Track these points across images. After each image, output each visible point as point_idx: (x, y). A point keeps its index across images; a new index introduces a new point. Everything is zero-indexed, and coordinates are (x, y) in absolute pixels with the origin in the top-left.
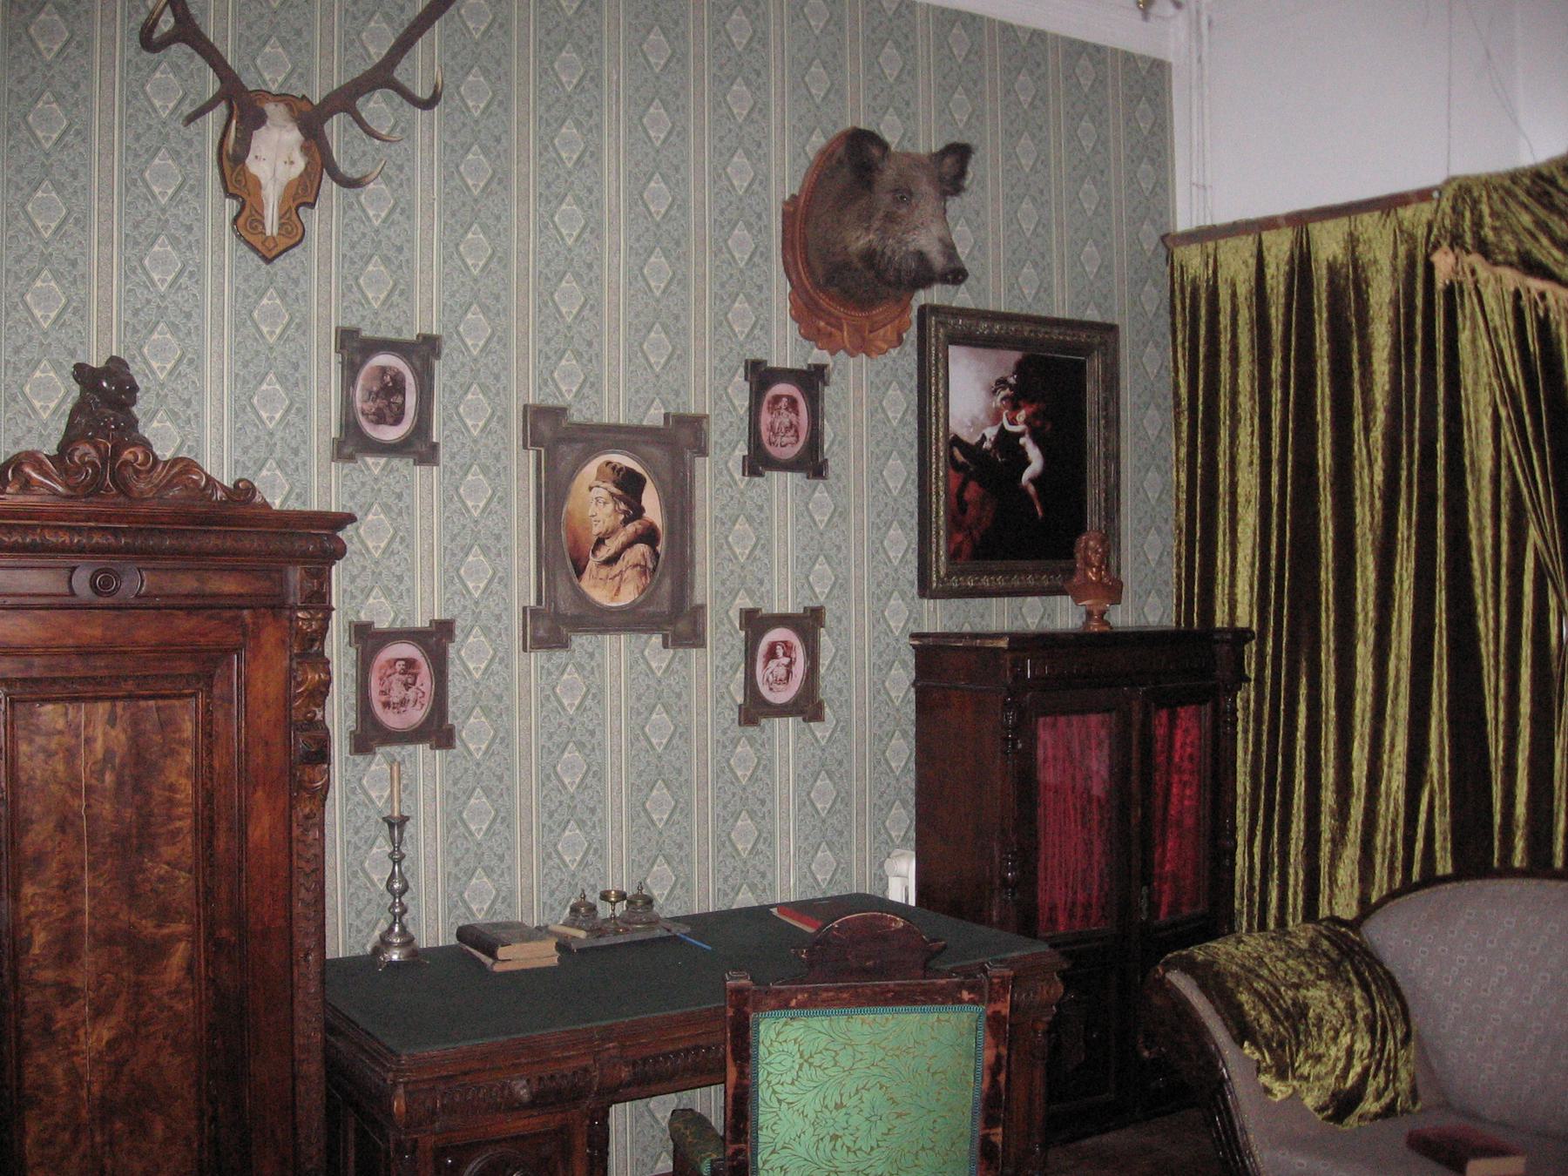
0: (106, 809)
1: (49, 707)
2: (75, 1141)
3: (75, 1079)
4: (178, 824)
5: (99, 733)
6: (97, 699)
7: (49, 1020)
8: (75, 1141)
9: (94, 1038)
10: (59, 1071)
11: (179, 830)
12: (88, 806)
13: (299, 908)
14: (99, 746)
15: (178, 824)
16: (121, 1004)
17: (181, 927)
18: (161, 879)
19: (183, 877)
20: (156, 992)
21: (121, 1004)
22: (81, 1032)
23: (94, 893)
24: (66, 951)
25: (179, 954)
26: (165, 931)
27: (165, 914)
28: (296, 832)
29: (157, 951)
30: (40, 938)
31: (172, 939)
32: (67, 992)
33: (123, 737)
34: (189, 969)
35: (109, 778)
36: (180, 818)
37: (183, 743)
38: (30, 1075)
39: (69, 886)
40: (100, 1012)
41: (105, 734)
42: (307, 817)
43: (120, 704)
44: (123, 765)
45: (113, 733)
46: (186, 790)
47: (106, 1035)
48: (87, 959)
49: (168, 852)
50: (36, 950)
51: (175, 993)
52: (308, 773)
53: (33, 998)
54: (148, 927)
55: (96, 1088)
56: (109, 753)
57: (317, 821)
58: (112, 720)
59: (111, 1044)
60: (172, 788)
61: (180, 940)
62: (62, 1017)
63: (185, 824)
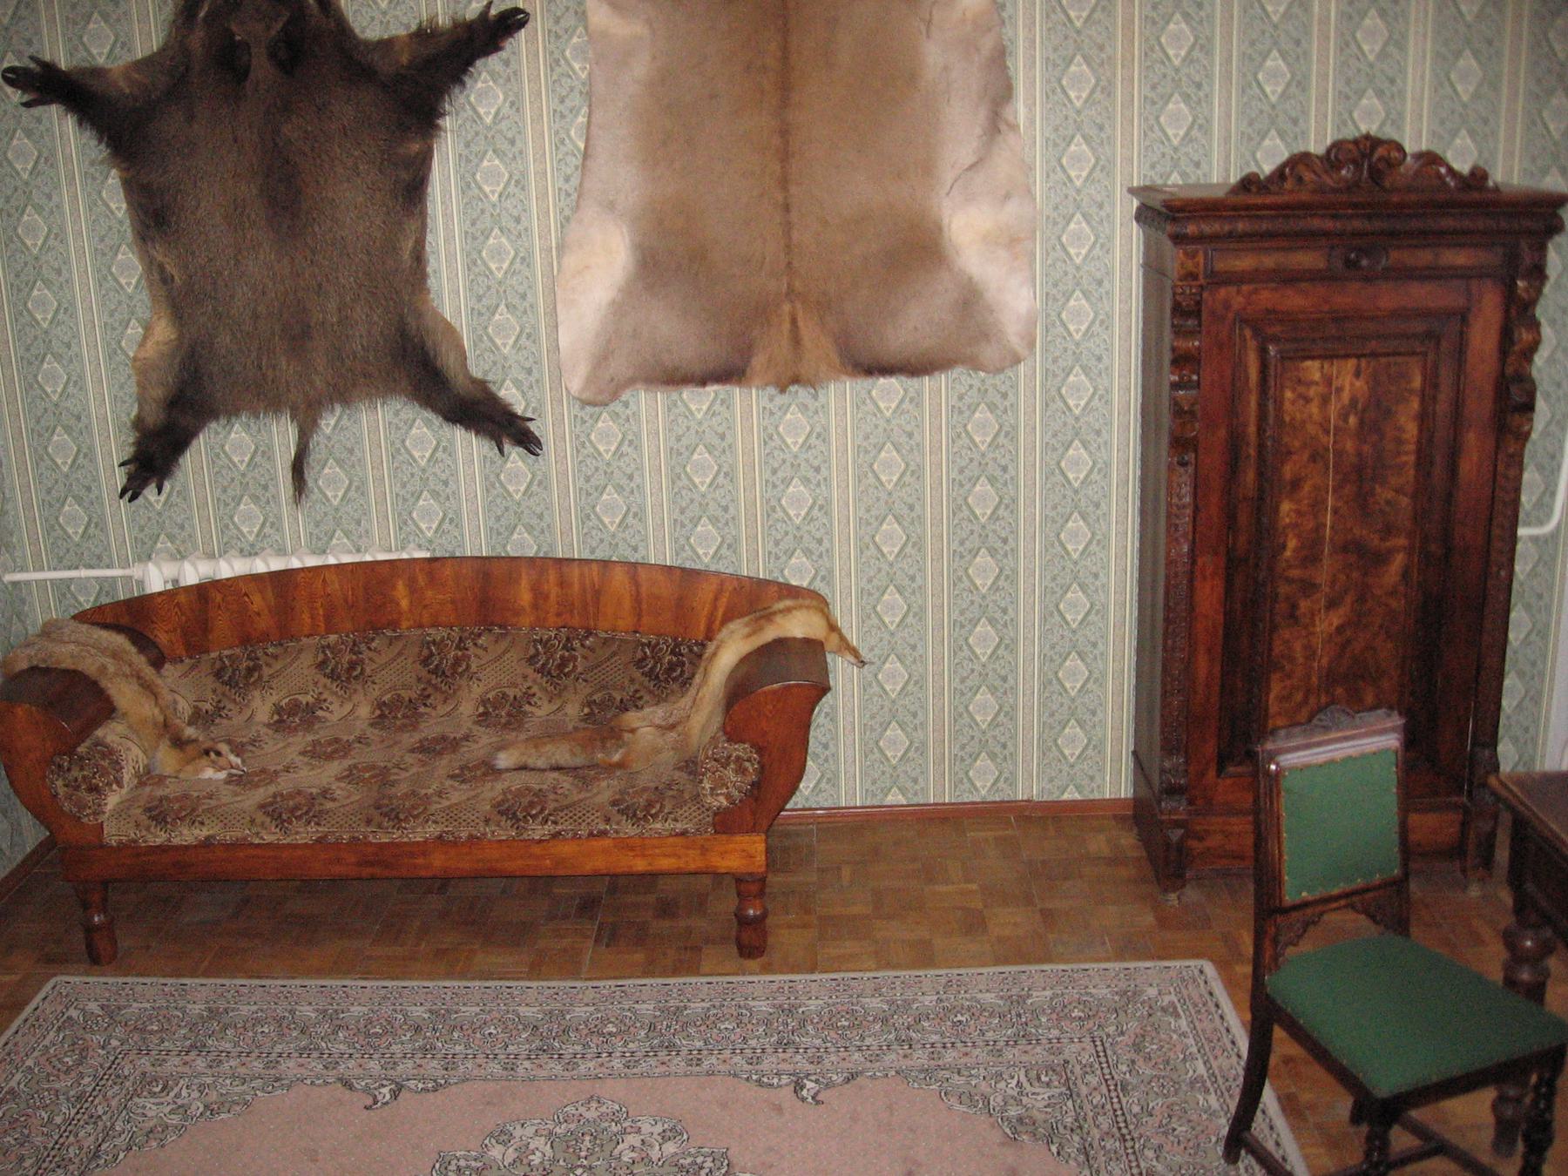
0: (1349, 445)
1: (1309, 363)
2: (1305, 701)
3: (1310, 652)
4: (1405, 458)
5: (1347, 388)
6: (1347, 356)
7: (1294, 606)
8: (1305, 701)
9: (1327, 623)
10: (1298, 646)
11: (1405, 463)
12: (1335, 442)
13: (1496, 531)
14: (1346, 396)
15: (1405, 458)
16: (1349, 599)
17: (1402, 541)
18: (1388, 502)
19: (1405, 501)
20: (1378, 592)
21: (1349, 599)
22: (1317, 619)
23: (1335, 511)
24: (1310, 556)
25: (1399, 560)
26: (1388, 544)
27: (1388, 531)
28: (1501, 468)
29: (1380, 559)
30: (1292, 543)
31: (1391, 552)
32: (1308, 587)
33: (1365, 388)
34: (1405, 575)
35: (1352, 420)
36: (1406, 453)
37: (1411, 392)
38: (1278, 647)
39: (1317, 505)
40: (1332, 605)
41: (1352, 385)
42: (1512, 456)
43: (1364, 363)
44: (1364, 410)
45: (1358, 384)
46: (1411, 430)
47: (1336, 622)
48: (1326, 561)
49: (1394, 481)
50: (1288, 553)
51: (1392, 593)
52: (1517, 418)
53: (1283, 589)
54: (1374, 541)
55: (1325, 661)
56: (1354, 401)
57: (1517, 463)
58: (1357, 374)
59: (1340, 630)
60: (1401, 429)
61: (1398, 551)
62: (1304, 605)
63: (1411, 458)
